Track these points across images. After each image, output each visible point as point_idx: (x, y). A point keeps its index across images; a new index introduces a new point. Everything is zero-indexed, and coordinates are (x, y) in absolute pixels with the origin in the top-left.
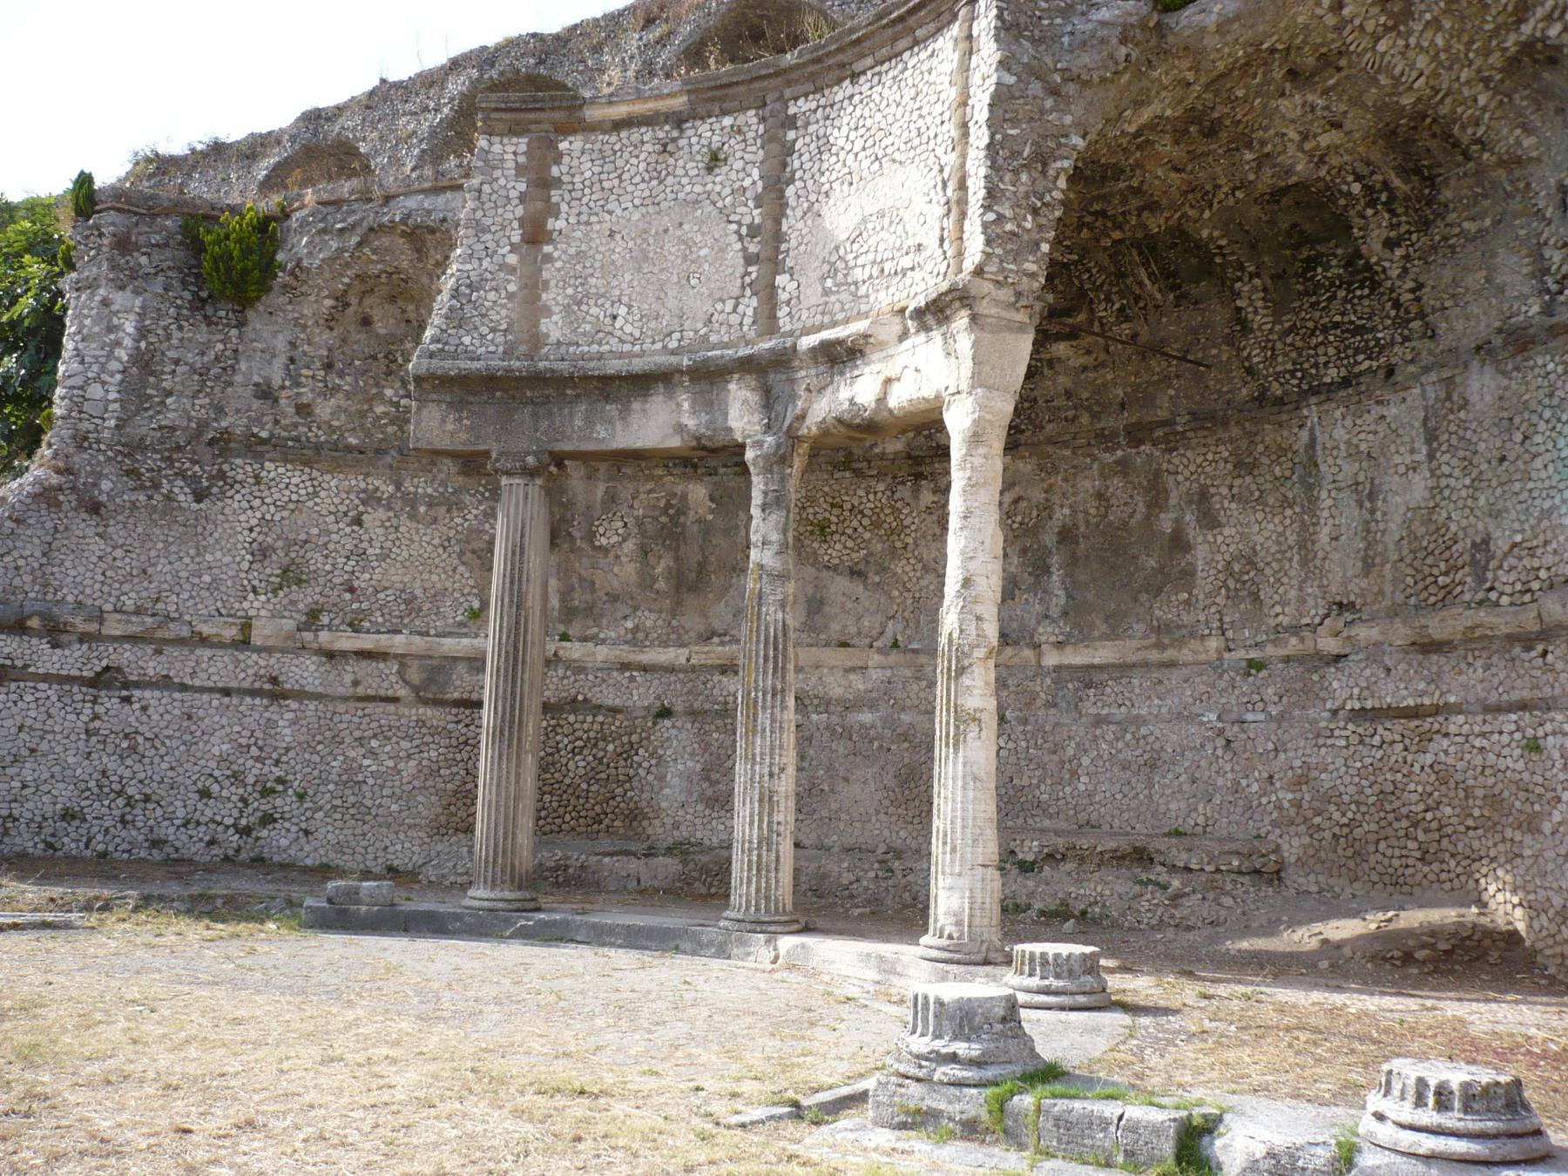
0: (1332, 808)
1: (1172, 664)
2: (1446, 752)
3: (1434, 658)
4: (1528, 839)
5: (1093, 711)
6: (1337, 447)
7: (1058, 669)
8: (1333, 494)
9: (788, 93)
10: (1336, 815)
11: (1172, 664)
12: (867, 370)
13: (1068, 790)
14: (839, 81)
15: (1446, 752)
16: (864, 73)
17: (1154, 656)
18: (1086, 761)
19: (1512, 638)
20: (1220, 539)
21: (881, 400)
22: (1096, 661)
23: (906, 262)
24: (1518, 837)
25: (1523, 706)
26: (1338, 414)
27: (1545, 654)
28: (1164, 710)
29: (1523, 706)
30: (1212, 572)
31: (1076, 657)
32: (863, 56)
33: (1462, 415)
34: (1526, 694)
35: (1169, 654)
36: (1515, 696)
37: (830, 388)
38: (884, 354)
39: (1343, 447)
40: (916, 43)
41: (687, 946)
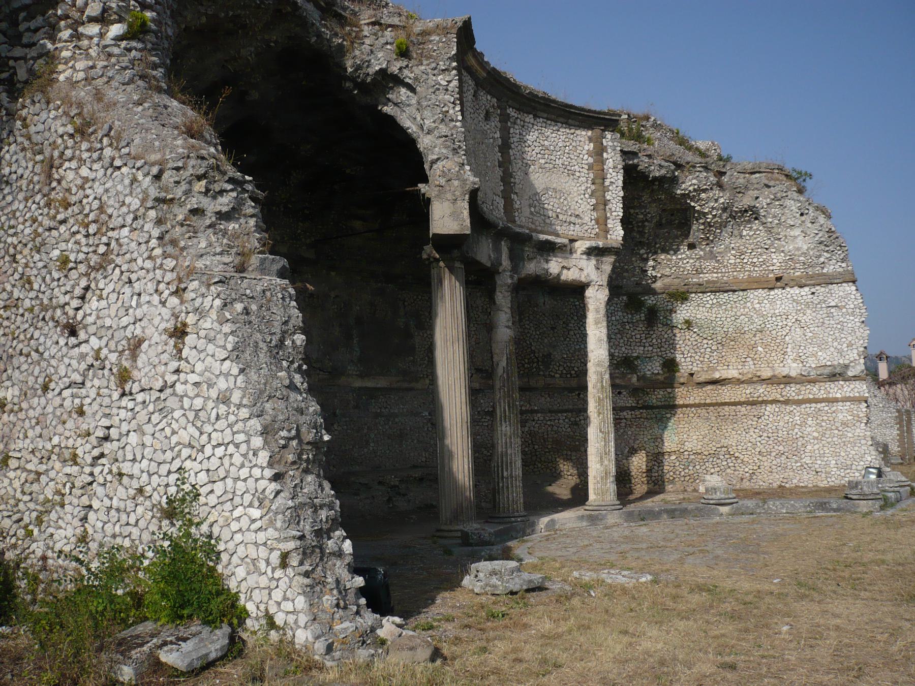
0: (483, 450)
1: (411, 389)
2: (534, 427)
3: (527, 393)
4: (574, 453)
5: (374, 410)
6: (478, 307)
7: (360, 388)
8: (476, 325)
9: (510, 102)
10: (485, 452)
11: (411, 389)
12: (554, 259)
13: (366, 450)
14: (529, 113)
15: (534, 427)
16: (539, 118)
17: (405, 385)
18: (372, 436)
19: (565, 389)
20: (425, 335)
21: (559, 275)
22: (379, 386)
23: (573, 219)
24: (569, 453)
25: (571, 411)
26: (478, 294)
27: (579, 394)
28: (405, 410)
29: (571, 411)
30: (423, 349)
31: (369, 384)
32: (544, 111)
33: (535, 309)
34: (571, 407)
35: (413, 385)
36: (566, 407)
37: (535, 260)
38: (563, 255)
39: (480, 308)
40: (566, 123)
41: (514, 534)
